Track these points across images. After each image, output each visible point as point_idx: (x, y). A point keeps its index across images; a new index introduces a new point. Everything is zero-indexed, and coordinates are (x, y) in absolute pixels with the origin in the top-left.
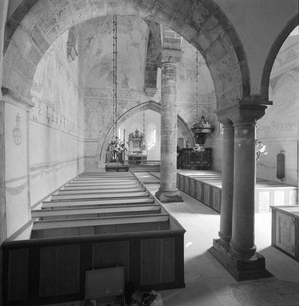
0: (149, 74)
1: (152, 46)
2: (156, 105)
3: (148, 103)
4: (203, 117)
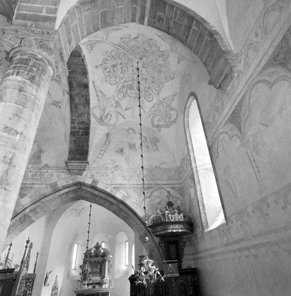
0: (75, 142)
1: (77, 101)
2: (89, 189)
3: (75, 188)
4: (170, 204)
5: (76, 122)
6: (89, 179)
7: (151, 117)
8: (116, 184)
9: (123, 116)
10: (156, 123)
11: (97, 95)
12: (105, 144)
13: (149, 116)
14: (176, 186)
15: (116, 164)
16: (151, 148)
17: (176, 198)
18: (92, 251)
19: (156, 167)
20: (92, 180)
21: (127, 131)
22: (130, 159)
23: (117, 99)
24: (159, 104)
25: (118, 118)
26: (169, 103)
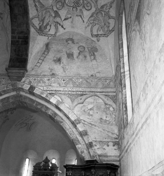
0: (15, 50)
1: (16, 11)
5: (16, 31)
6: (27, 85)
7: (90, 27)
8: (52, 91)
9: (62, 27)
10: (95, 33)
11: (36, 5)
12: (44, 53)
13: (88, 26)
14: (110, 94)
15: (54, 72)
16: (88, 57)
17: (109, 105)
18: (42, 165)
19: (92, 76)
20: (29, 86)
21: (67, 41)
22: (67, 68)
23: (55, 9)
24: (97, 13)
25: (57, 29)
26: (107, 10)
